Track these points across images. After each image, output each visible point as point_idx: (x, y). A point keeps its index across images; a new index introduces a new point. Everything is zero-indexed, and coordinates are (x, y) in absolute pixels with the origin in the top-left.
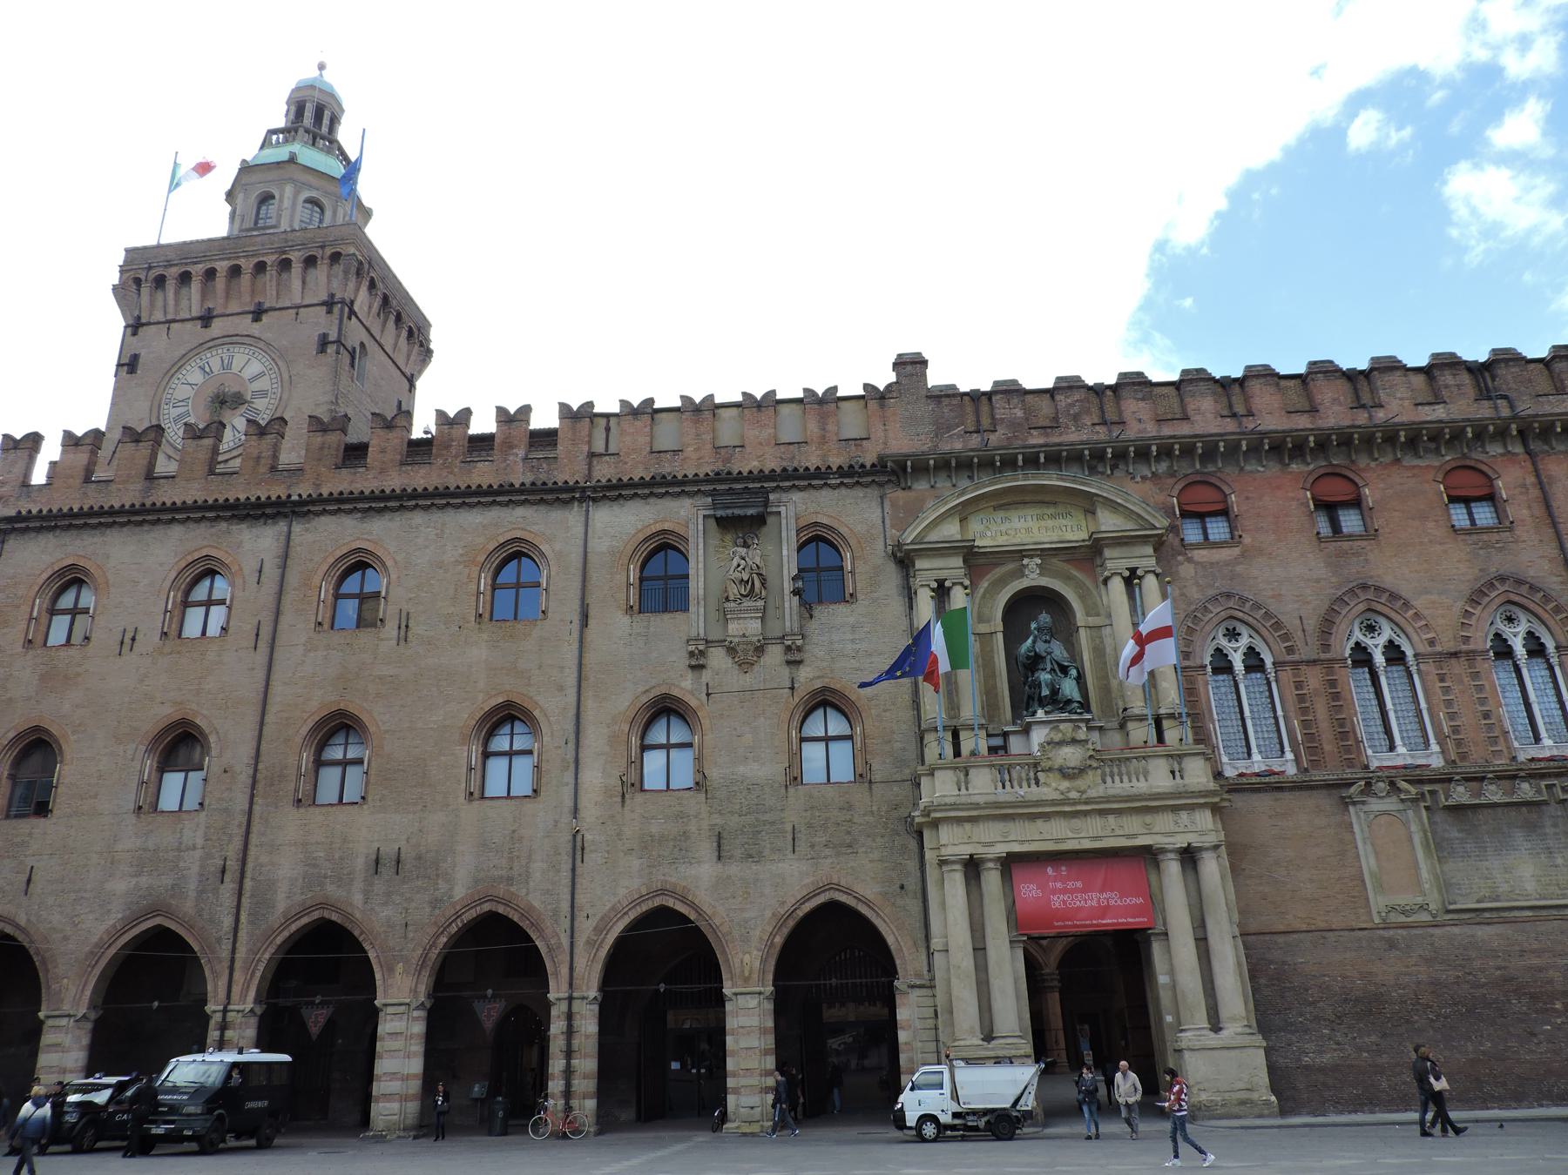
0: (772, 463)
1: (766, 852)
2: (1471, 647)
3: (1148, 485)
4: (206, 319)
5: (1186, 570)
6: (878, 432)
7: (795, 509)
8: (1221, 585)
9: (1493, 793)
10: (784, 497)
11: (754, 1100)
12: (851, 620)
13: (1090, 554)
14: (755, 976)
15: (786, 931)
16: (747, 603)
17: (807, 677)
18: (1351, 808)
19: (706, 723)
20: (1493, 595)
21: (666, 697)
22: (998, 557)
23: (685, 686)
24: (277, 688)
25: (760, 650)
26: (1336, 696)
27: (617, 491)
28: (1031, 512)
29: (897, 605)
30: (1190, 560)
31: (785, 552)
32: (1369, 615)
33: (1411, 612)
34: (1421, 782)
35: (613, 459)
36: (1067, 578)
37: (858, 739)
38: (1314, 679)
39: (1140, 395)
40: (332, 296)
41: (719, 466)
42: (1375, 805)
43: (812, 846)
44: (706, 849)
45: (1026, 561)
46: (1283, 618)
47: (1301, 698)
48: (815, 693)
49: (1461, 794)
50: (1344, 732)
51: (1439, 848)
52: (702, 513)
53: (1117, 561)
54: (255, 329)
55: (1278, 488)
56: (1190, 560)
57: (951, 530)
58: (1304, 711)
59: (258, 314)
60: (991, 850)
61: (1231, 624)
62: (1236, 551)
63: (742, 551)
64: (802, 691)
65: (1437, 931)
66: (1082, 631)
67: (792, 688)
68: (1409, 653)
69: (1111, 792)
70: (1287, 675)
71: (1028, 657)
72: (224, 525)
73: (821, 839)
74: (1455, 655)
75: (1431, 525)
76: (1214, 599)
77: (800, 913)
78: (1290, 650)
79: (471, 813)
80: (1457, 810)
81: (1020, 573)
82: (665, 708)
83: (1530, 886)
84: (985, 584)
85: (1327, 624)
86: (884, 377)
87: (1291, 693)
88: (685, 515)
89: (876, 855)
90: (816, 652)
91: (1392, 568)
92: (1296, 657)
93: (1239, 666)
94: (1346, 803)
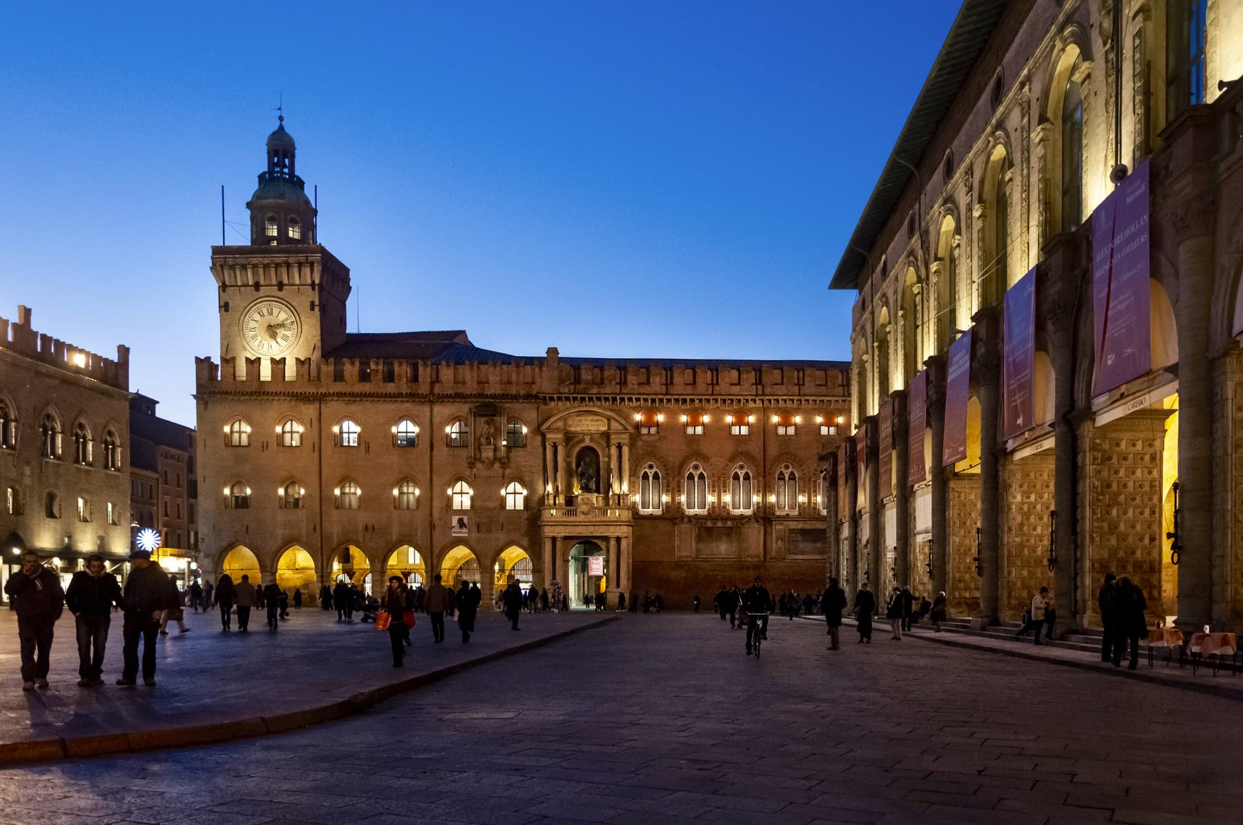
4: (257, 286)
5: (640, 443)
6: (538, 381)
9: (719, 524)
13: (606, 436)
22: (575, 434)
24: (324, 468)
25: (493, 464)
27: (443, 398)
28: (590, 418)
29: (541, 450)
40: (313, 282)
49: (709, 524)
51: (699, 539)
53: (614, 440)
54: (280, 294)
59: (281, 286)
72: (293, 403)
79: (396, 514)
80: (709, 530)
85: (682, 466)
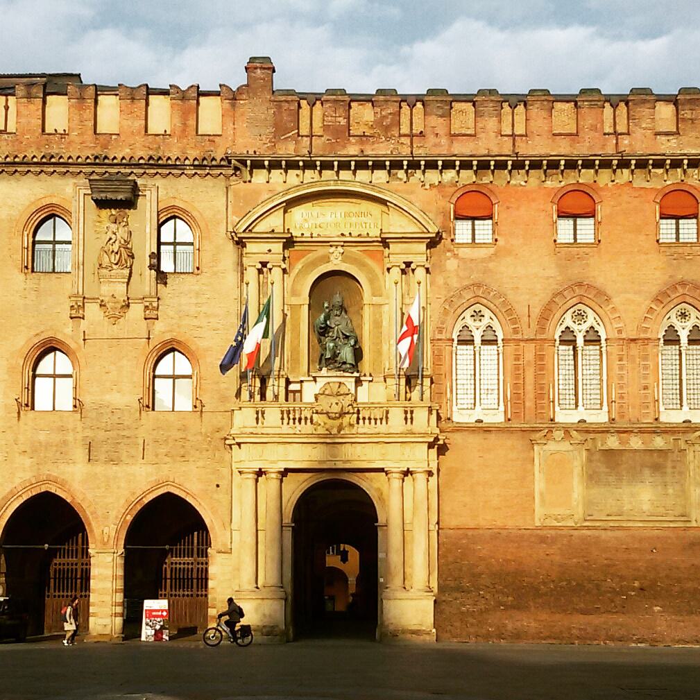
0: (141, 153)
1: (124, 456)
2: (648, 336)
3: (435, 190)
5: (451, 264)
7: (157, 192)
8: (475, 277)
9: (636, 443)
10: (150, 182)
11: (107, 621)
12: (197, 288)
14: (111, 542)
15: (135, 513)
16: (117, 270)
17: (161, 331)
18: (536, 447)
19: (82, 361)
20: (673, 296)
21: (51, 339)
23: (66, 331)
26: (542, 367)
29: (232, 277)
30: (456, 256)
31: (148, 230)
32: (580, 306)
33: (611, 306)
34: (588, 432)
35: (10, 138)
36: (362, 265)
37: (194, 378)
38: (529, 352)
39: (440, 112)
41: (97, 151)
42: (552, 446)
43: (157, 455)
44: (80, 454)
45: (333, 248)
46: (516, 306)
47: (517, 368)
48: (166, 343)
49: (613, 442)
50: (542, 394)
51: (592, 478)
52: (82, 192)
53: (398, 255)
55: (534, 200)
56: (456, 256)
57: (274, 222)
58: (517, 377)
60: (274, 466)
61: (478, 307)
62: (492, 250)
63: (113, 227)
64: (153, 343)
65: (575, 533)
66: (366, 308)
67: (149, 338)
68: (603, 337)
69: (361, 431)
70: (511, 348)
71: (321, 328)
73: (163, 450)
74: (633, 340)
75: (642, 238)
76: (467, 288)
77: (146, 501)
78: (516, 331)
80: (609, 453)
81: (326, 259)
82: (49, 348)
83: (646, 507)
84: (299, 266)
86: (237, 79)
87: (510, 363)
88: (70, 191)
89: (201, 464)
90: (167, 309)
91: (603, 272)
92: (519, 336)
93: (478, 340)
94: (532, 443)
